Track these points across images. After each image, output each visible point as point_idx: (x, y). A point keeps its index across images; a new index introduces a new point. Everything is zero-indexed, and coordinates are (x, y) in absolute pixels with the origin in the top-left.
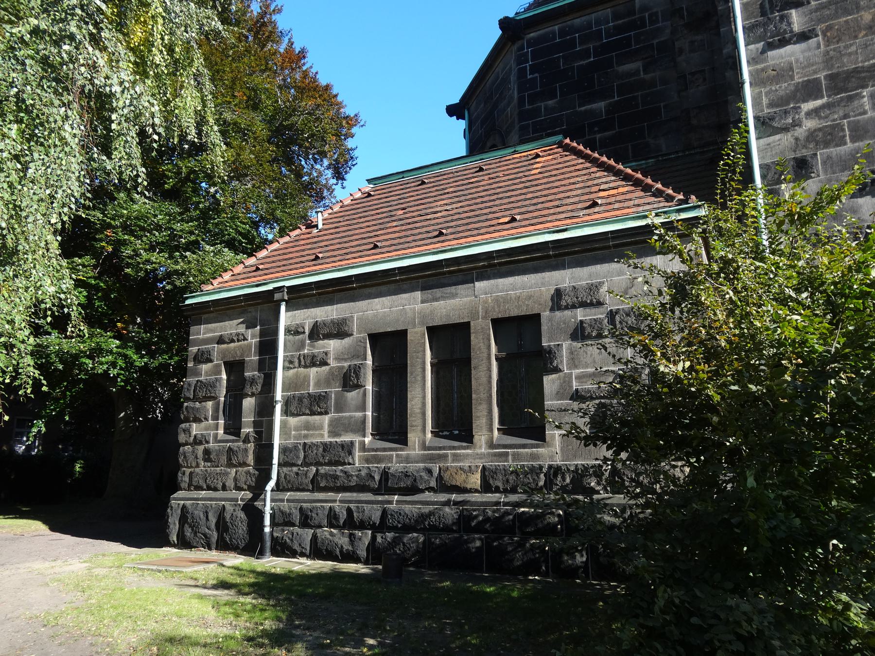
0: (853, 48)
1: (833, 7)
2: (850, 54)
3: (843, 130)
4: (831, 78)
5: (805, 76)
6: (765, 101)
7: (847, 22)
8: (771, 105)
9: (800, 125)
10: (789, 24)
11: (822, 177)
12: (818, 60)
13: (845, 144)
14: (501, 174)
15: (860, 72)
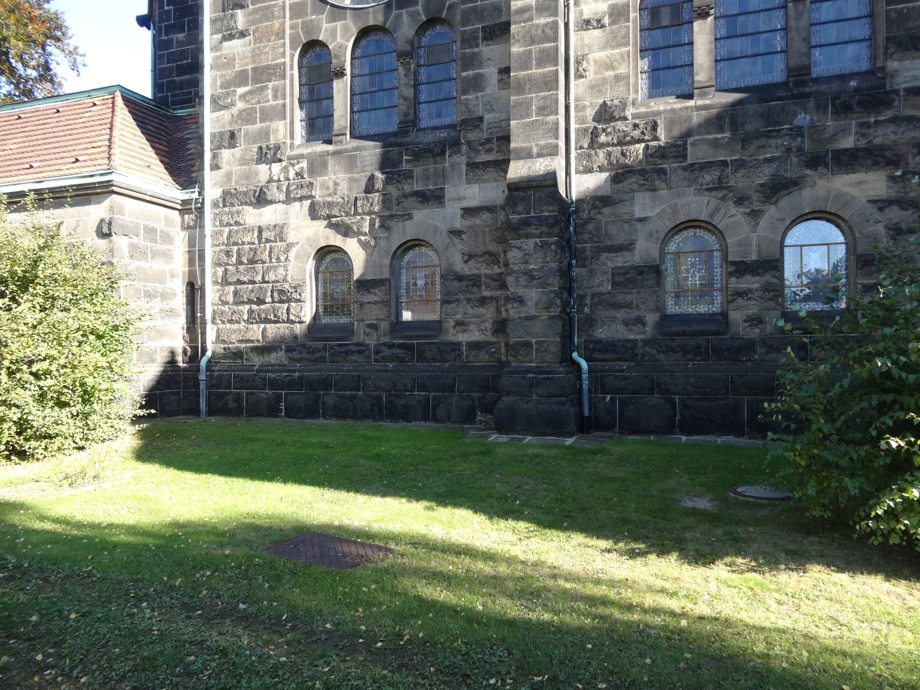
0: (267, 49)
1: (260, 13)
2: (265, 53)
3: (256, 112)
4: (255, 70)
5: (242, 66)
6: (219, 83)
7: (266, 26)
8: (222, 87)
9: (234, 105)
10: (235, 22)
11: (243, 147)
12: (249, 54)
13: (255, 123)
14: (63, 119)
15: (269, 69)
